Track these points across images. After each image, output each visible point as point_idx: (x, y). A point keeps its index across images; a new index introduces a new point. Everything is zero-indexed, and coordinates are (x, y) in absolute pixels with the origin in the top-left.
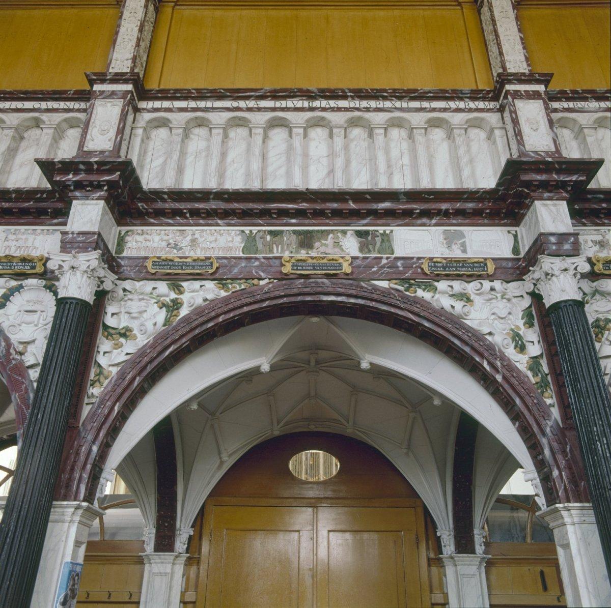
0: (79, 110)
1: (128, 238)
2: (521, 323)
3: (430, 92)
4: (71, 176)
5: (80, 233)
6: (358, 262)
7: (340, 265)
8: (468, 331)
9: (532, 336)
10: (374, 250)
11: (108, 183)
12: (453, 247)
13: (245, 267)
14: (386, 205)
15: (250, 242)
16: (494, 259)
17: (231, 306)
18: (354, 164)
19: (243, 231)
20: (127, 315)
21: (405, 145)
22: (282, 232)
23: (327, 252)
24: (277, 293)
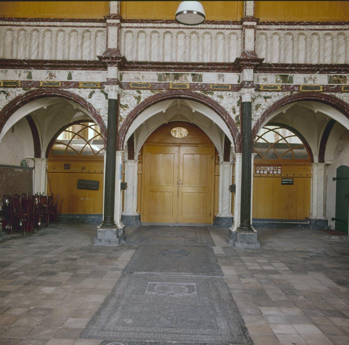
0: (101, 27)
1: (123, 75)
2: (236, 105)
3: (219, 22)
4: (107, 60)
5: (112, 79)
6: (192, 85)
7: (186, 86)
8: (221, 107)
9: (238, 109)
10: (197, 81)
11: (118, 62)
12: (220, 80)
13: (159, 86)
14: (201, 66)
15: (160, 78)
16: (231, 85)
17: (155, 98)
18: (192, 49)
19: (157, 73)
20: (126, 101)
21: (209, 41)
22: (169, 74)
23: (183, 81)
24: (168, 94)
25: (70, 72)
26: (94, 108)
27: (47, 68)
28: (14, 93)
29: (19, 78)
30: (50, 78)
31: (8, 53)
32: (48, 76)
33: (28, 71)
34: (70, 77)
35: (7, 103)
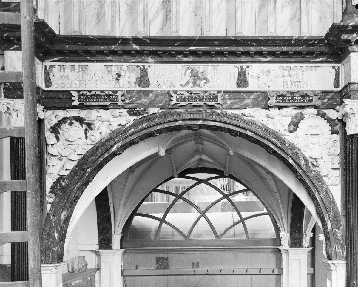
25: (242, 68)
26: (304, 157)
27: (185, 59)
28: (107, 123)
29: (117, 85)
30: (195, 84)
31: (88, 23)
32: (187, 78)
33: (138, 67)
34: (242, 80)
35: (90, 147)
